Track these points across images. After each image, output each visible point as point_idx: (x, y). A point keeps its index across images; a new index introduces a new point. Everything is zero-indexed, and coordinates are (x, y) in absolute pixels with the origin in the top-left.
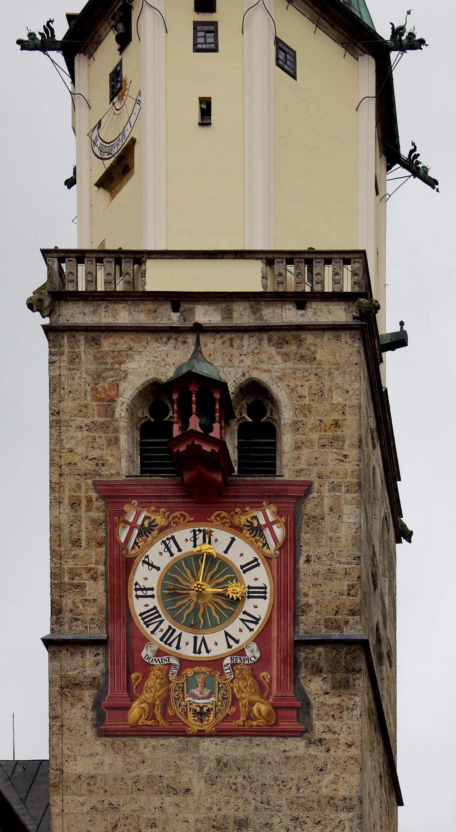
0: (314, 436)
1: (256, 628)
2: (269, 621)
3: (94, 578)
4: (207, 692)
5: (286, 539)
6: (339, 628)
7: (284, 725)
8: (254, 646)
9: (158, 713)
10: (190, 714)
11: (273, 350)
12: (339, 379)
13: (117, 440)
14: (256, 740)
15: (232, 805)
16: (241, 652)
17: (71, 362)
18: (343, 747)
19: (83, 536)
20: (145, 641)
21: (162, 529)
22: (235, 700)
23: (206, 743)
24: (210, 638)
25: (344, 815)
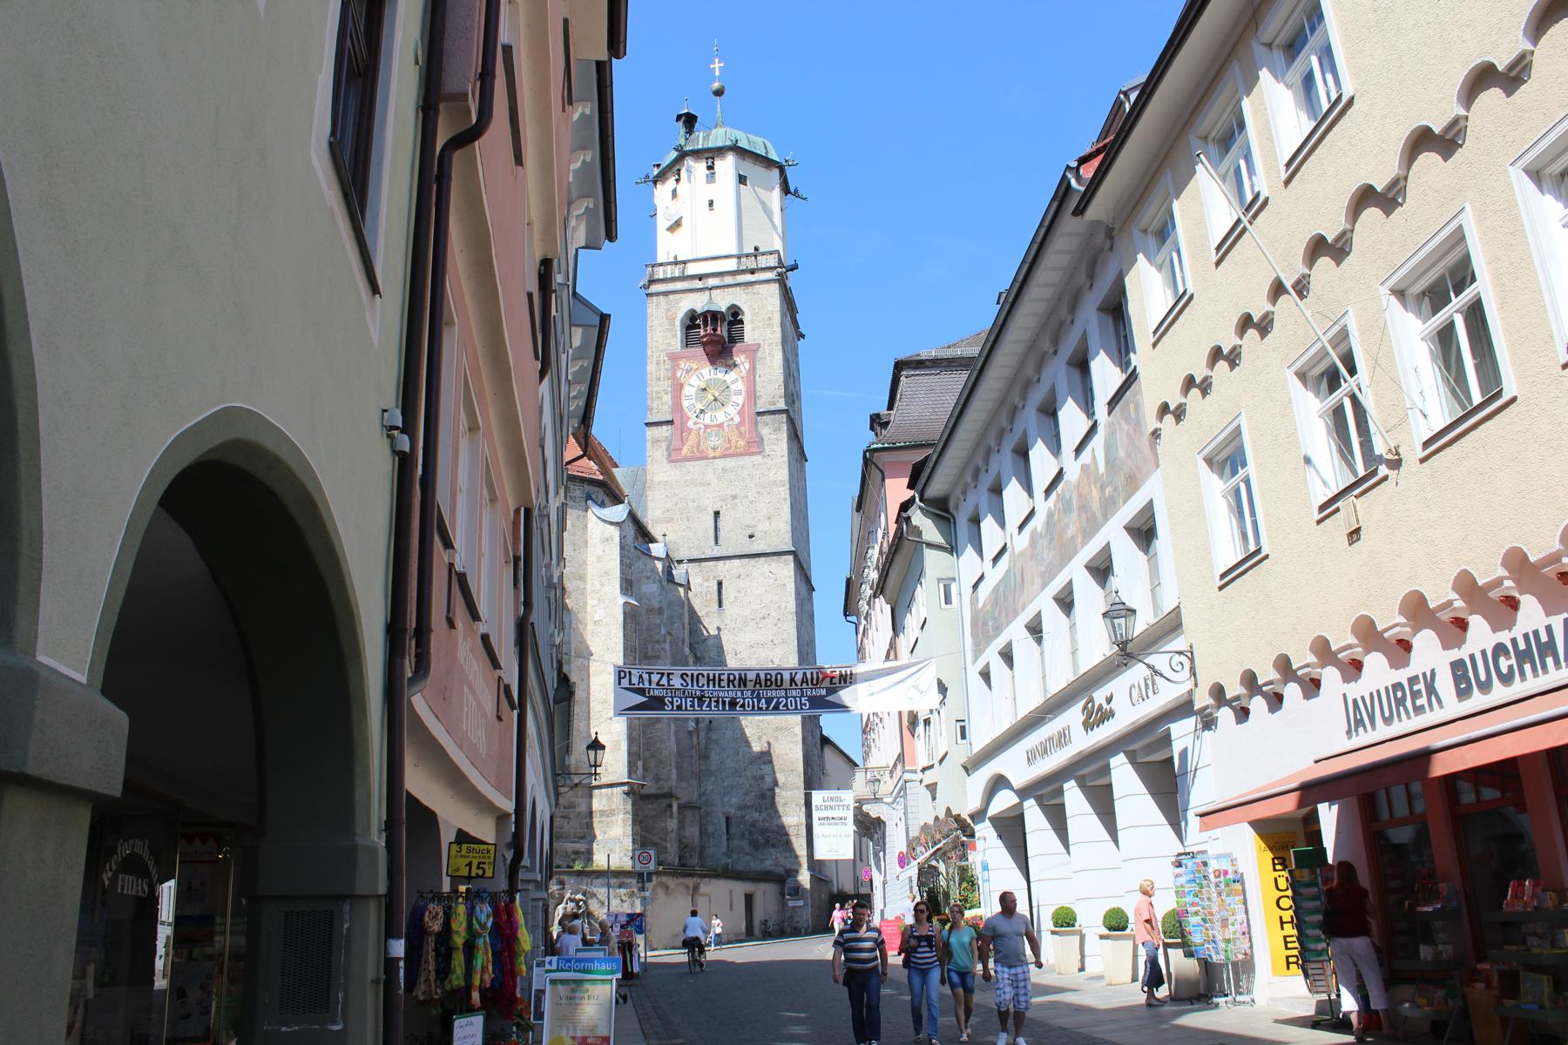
0: (760, 325)
1: (738, 408)
2: (743, 406)
3: (667, 394)
4: (717, 439)
5: (749, 370)
6: (775, 404)
7: (752, 450)
8: (737, 416)
9: (695, 449)
10: (710, 449)
11: (742, 292)
12: (770, 300)
13: (676, 334)
14: (739, 458)
15: (729, 489)
16: (732, 419)
17: (657, 305)
18: (779, 457)
19: (662, 376)
20: (689, 418)
21: (697, 369)
22: (729, 440)
23: (717, 461)
24: (718, 415)
25: (780, 489)
